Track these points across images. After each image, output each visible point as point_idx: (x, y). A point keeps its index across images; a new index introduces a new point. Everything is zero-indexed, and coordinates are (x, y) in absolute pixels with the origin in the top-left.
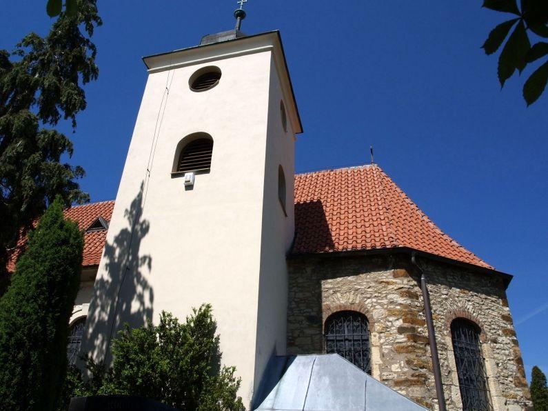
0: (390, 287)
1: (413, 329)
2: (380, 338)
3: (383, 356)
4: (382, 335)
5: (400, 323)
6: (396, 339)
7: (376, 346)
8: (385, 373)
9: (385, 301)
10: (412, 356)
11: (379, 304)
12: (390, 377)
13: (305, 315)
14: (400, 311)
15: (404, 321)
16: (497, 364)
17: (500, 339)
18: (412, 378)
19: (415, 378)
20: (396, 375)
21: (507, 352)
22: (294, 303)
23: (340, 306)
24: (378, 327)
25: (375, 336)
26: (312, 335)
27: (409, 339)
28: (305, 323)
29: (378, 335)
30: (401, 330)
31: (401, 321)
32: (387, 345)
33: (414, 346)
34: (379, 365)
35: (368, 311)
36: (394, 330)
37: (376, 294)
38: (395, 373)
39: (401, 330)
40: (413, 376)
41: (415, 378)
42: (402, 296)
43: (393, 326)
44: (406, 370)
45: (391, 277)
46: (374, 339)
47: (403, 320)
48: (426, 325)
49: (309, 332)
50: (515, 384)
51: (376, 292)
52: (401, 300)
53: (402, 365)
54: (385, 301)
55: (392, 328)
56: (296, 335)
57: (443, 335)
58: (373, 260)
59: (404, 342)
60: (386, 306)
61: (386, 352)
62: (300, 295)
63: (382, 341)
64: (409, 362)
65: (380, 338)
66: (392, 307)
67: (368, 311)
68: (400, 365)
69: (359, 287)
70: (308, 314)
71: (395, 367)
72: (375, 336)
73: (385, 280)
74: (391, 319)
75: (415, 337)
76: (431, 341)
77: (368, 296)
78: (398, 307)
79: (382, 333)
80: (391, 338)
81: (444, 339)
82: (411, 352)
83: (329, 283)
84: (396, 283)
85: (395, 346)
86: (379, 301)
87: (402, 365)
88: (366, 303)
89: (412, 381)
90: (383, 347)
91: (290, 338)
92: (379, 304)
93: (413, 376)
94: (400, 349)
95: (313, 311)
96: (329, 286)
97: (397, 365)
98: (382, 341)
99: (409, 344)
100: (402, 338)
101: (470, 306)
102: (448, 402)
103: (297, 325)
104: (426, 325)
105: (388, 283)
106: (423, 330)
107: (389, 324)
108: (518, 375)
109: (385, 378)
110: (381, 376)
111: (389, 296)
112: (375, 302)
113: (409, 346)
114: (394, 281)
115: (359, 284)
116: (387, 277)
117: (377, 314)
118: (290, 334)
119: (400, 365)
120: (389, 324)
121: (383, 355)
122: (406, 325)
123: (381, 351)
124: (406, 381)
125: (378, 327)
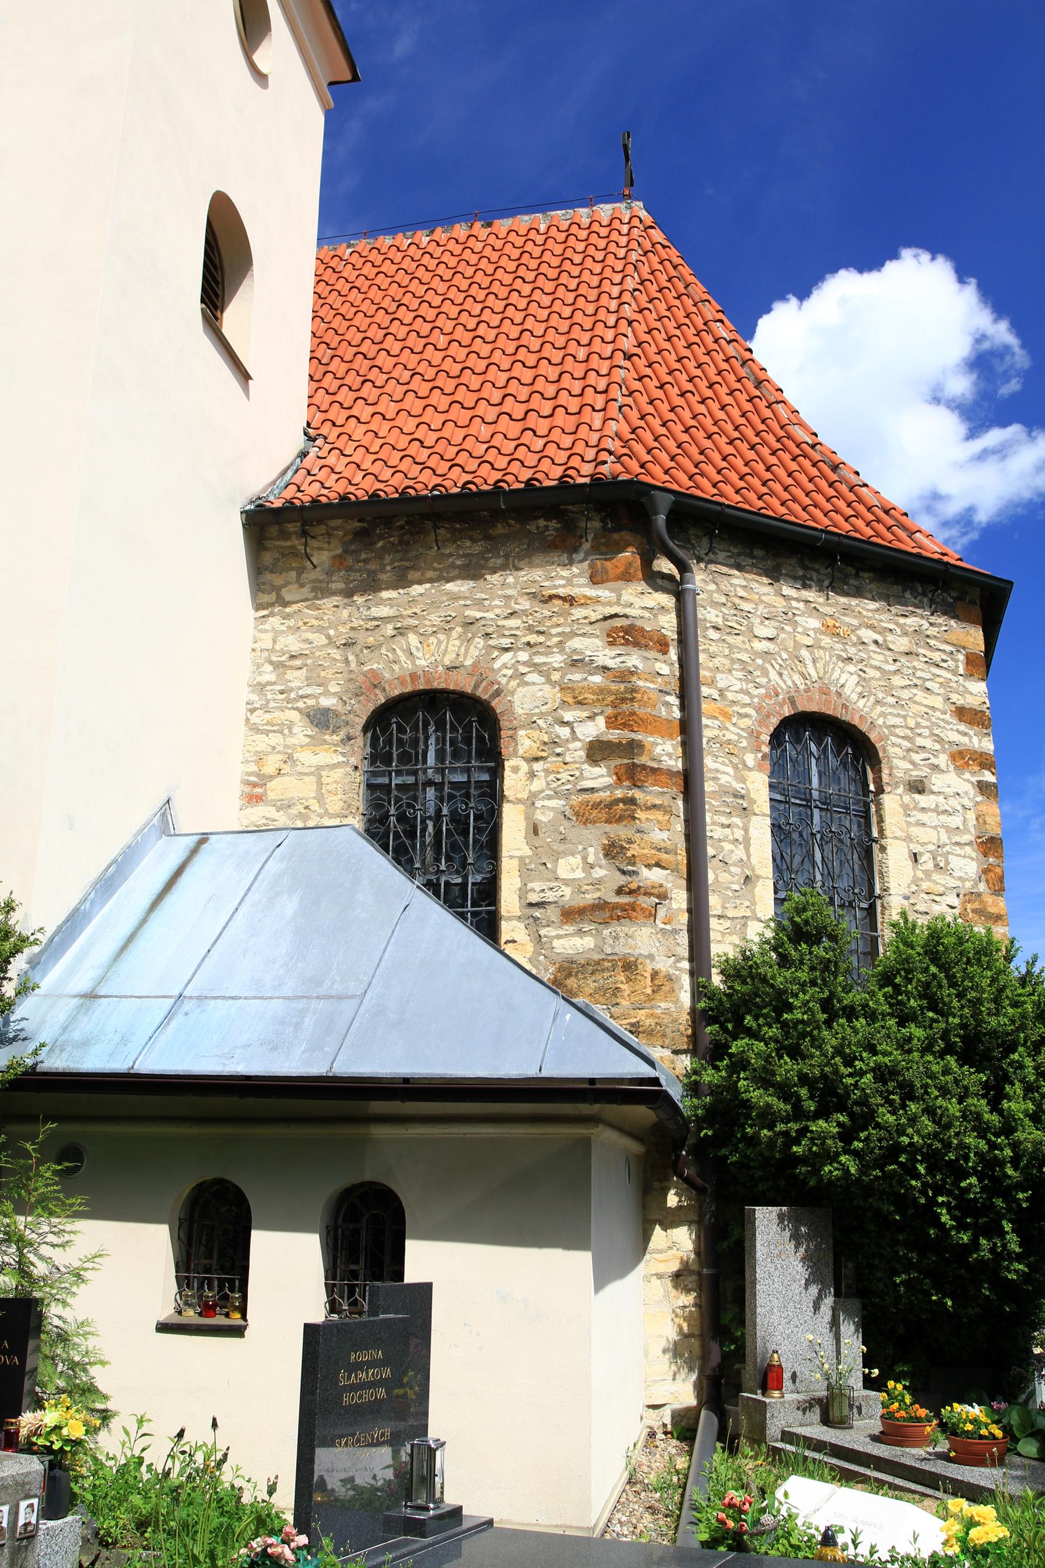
0: (578, 613)
1: (633, 747)
2: (532, 775)
3: (536, 832)
4: (537, 766)
5: (595, 729)
6: (582, 777)
7: (519, 801)
8: (537, 885)
9: (557, 659)
10: (621, 831)
12: (550, 896)
13: (300, 704)
14: (601, 691)
15: (612, 722)
20: (567, 891)
22: (268, 668)
23: (414, 676)
25: (516, 769)
26: (319, 768)
28: (302, 731)
29: (524, 767)
30: (597, 751)
31: (601, 721)
34: (521, 859)
36: (576, 752)
37: (533, 638)
38: (566, 882)
39: (597, 751)
40: (619, 891)
42: (611, 644)
44: (599, 873)
45: (583, 581)
47: (608, 718)
49: (308, 758)
51: (530, 629)
52: (607, 656)
55: (572, 746)
56: (269, 769)
58: (532, 527)
59: (608, 787)
61: (543, 817)
62: (292, 643)
63: (537, 785)
64: (613, 851)
65: (532, 775)
66: (577, 677)
67: (498, 693)
69: (478, 615)
70: (311, 702)
71: (569, 867)
73: (561, 592)
77: (505, 642)
78: (597, 679)
79: (537, 759)
82: (620, 819)
83: (382, 602)
84: (597, 600)
85: (577, 799)
86: (538, 659)
88: (497, 665)
89: (616, 906)
90: (538, 804)
91: (253, 779)
92: (536, 667)
93: (619, 891)
95: (327, 693)
96: (384, 611)
97: (576, 861)
98: (537, 785)
99: (619, 793)
103: (275, 739)
105: (570, 600)
109: (534, 898)
110: (523, 892)
112: (525, 663)
114: (592, 592)
115: (479, 604)
116: (569, 582)
118: (253, 768)
119: (585, 859)
120: (564, 732)
121: (535, 830)
122: (615, 735)
123: (528, 818)
124: (600, 906)
125: (528, 743)
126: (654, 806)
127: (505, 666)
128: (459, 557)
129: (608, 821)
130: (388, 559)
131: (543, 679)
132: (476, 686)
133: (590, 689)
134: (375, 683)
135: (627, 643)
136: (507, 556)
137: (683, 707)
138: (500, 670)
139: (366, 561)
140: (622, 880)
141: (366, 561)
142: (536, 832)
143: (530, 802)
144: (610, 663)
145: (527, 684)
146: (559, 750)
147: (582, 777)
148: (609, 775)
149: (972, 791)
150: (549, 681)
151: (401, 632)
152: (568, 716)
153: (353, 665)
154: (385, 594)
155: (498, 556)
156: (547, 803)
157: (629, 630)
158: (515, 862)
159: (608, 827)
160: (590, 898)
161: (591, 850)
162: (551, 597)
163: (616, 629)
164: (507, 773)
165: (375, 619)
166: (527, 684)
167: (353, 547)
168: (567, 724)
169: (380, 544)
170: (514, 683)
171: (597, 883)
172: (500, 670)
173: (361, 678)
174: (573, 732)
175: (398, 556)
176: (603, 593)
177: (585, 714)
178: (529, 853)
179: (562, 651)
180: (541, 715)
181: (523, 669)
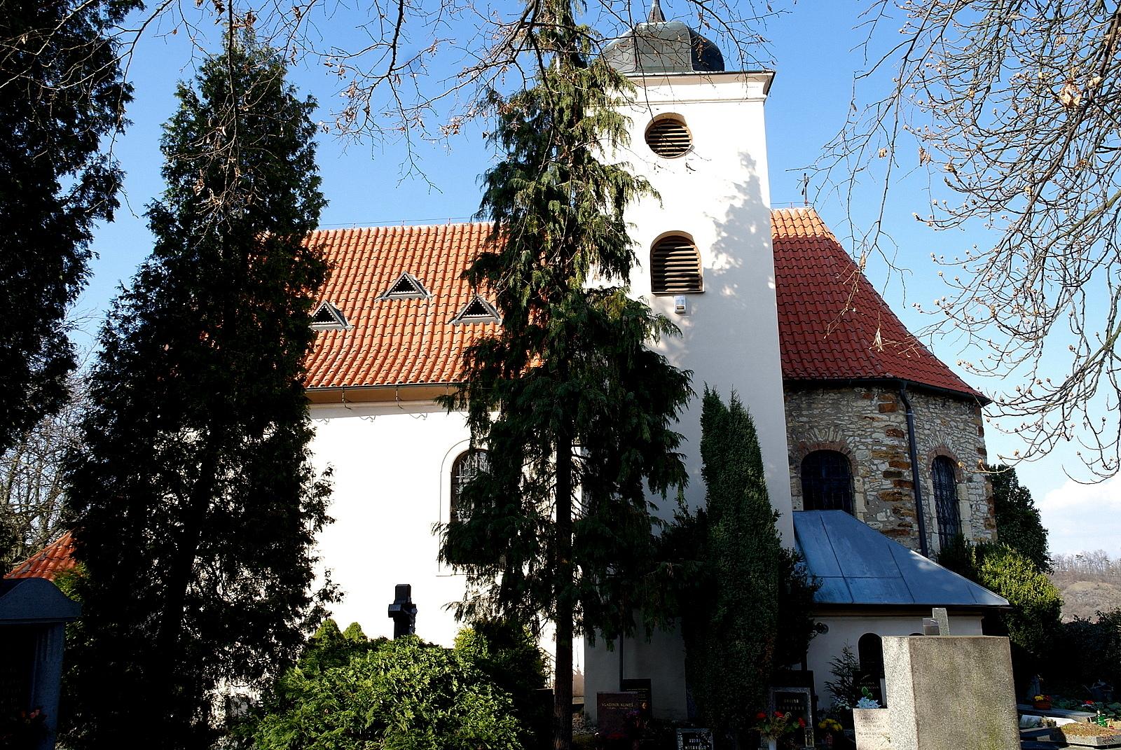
0: (875, 424)
1: (900, 474)
2: (864, 483)
3: (868, 504)
4: (866, 480)
5: (885, 467)
6: (882, 485)
10: (898, 504)
11: (863, 444)
15: (891, 464)
16: (971, 506)
17: (975, 478)
18: (899, 528)
19: (901, 528)
20: (882, 525)
21: (980, 492)
23: (819, 445)
24: (861, 471)
25: (859, 481)
27: (895, 486)
30: (887, 475)
31: (887, 463)
32: (871, 491)
33: (900, 493)
34: (864, 513)
35: (850, 452)
39: (887, 475)
40: (899, 525)
41: (901, 528)
43: (878, 470)
44: (892, 519)
46: (858, 484)
48: (910, 469)
50: (985, 526)
52: (889, 441)
53: (889, 514)
54: (869, 440)
57: (925, 478)
59: (890, 489)
60: (870, 447)
61: (870, 498)
63: (866, 487)
64: (896, 511)
65: (864, 483)
66: (878, 447)
67: (850, 452)
68: (886, 513)
69: (840, 422)
71: (881, 516)
72: (859, 481)
73: (869, 415)
74: (876, 462)
75: (900, 483)
76: (915, 485)
77: (851, 433)
78: (884, 448)
79: (865, 477)
80: (876, 484)
81: (926, 482)
83: (803, 416)
85: (880, 492)
86: (862, 440)
87: (889, 514)
89: (899, 530)
90: (868, 493)
92: (863, 444)
93: (899, 525)
94: (885, 496)
96: (805, 419)
98: (866, 487)
99: (895, 491)
100: (888, 484)
101: (949, 442)
102: (929, 551)
104: (910, 469)
105: (873, 419)
106: (907, 475)
107: (875, 467)
108: (989, 516)
111: (873, 436)
112: (858, 442)
113: (896, 493)
114: (880, 416)
115: (839, 419)
117: (860, 454)
120: (875, 467)
121: (867, 503)
122: (892, 469)
123: (865, 498)
126: (906, 495)
127: (851, 442)
128: (830, 400)
129: (893, 501)
130: (803, 399)
131: (865, 448)
132: (841, 449)
133: (882, 451)
134: (804, 447)
135: (894, 436)
136: (848, 401)
137: (911, 458)
138: (849, 444)
139: (795, 399)
140: (899, 522)
141: (795, 399)
142: (868, 502)
143: (865, 493)
144: (889, 443)
145: (860, 449)
146: (873, 474)
147: (882, 485)
148: (891, 484)
149: (983, 479)
150: (867, 448)
151: (811, 428)
152: (876, 462)
153: (795, 439)
154: (804, 413)
155: (844, 401)
156: (870, 493)
157: (894, 430)
158: (862, 514)
159: (893, 502)
160: (890, 527)
161: (888, 511)
162: (866, 417)
163: (889, 430)
164: (855, 482)
165: (802, 422)
166: (860, 449)
167: (790, 394)
168: (876, 465)
169: (800, 393)
170: (855, 449)
171: (891, 523)
172: (849, 444)
173: (799, 445)
174: (877, 468)
175: (807, 398)
176: (884, 417)
177: (882, 461)
178: (866, 511)
179: (871, 438)
180: (866, 461)
181: (857, 444)
